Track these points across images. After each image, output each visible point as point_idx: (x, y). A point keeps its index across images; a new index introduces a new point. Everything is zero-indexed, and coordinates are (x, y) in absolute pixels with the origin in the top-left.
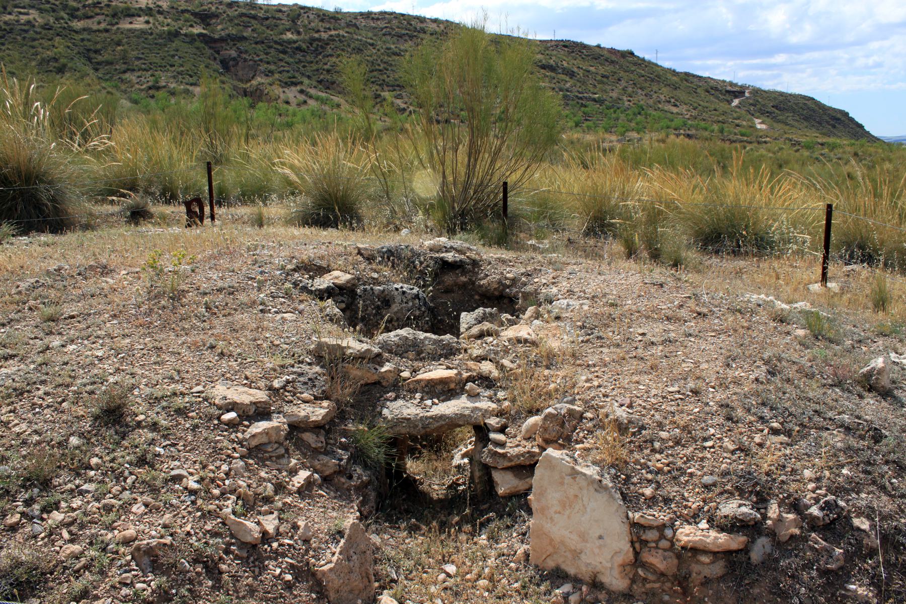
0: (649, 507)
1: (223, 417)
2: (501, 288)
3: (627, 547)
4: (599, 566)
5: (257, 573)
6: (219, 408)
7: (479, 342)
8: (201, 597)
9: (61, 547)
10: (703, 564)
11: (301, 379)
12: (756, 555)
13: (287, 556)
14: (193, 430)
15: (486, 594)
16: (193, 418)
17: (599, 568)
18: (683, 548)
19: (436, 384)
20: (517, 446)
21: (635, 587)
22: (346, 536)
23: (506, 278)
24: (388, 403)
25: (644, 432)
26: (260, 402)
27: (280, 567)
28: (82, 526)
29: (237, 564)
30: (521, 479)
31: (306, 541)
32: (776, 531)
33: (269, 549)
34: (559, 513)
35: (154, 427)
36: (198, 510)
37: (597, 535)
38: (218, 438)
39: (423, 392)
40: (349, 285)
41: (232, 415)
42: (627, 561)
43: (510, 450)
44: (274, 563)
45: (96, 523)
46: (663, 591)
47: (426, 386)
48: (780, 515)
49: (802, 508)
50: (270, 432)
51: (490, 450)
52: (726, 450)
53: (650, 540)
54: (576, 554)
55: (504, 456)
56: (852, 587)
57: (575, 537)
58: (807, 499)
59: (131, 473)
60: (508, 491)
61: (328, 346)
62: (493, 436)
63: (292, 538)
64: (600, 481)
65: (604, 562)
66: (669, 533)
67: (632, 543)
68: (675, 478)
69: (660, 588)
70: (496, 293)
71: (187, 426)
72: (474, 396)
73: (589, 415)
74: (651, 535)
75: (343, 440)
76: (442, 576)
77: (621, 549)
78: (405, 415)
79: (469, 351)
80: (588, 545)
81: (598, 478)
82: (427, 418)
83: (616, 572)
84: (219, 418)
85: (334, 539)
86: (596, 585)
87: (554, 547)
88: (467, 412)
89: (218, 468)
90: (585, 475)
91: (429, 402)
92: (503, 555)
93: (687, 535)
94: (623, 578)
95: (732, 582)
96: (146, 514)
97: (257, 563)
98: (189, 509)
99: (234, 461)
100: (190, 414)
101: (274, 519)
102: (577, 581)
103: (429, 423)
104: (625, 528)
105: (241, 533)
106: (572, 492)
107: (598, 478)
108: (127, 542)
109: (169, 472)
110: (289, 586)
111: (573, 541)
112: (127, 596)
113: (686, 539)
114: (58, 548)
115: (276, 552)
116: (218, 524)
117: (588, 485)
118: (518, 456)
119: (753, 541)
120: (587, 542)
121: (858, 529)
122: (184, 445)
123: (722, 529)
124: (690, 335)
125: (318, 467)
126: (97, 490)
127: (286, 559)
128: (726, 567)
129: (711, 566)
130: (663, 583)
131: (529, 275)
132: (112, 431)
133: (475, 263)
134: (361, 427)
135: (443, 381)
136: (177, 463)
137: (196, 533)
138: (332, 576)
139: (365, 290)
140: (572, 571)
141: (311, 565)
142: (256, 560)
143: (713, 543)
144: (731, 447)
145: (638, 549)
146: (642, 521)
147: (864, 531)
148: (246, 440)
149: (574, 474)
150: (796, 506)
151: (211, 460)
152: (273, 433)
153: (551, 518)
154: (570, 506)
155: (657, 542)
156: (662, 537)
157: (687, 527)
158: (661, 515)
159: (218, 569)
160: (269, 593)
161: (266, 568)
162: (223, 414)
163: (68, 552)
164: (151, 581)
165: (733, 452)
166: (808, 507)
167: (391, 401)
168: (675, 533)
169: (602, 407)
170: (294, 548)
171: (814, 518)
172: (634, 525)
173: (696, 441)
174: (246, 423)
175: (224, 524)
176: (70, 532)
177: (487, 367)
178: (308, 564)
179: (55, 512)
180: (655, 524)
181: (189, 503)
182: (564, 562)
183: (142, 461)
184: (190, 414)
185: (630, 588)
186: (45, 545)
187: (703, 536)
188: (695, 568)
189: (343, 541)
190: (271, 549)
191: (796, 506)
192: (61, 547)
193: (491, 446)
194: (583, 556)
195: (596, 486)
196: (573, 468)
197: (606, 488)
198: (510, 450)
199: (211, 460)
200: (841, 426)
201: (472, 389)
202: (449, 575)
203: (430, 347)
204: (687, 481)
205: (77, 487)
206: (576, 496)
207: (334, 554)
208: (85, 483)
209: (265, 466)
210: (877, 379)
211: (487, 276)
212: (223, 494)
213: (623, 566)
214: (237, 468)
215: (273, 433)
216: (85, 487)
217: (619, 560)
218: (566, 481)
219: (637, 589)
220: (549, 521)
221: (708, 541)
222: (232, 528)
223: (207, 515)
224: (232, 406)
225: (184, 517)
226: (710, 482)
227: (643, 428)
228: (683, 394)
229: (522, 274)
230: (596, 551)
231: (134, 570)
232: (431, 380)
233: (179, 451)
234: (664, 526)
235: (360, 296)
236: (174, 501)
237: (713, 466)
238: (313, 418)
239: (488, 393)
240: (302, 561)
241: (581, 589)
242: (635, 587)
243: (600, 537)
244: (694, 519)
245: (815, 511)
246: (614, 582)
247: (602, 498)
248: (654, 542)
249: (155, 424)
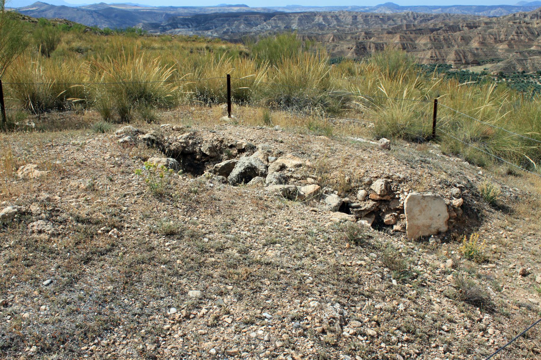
54: (429, 226)
57: (428, 220)
83: (444, 225)
86: (438, 233)
106: (424, 205)
111: (427, 222)
149: (424, 197)
154: (424, 210)
185: (448, 228)
194: (433, 226)
196: (423, 196)
217: (446, 220)
229: (187, 138)
243: (439, 215)
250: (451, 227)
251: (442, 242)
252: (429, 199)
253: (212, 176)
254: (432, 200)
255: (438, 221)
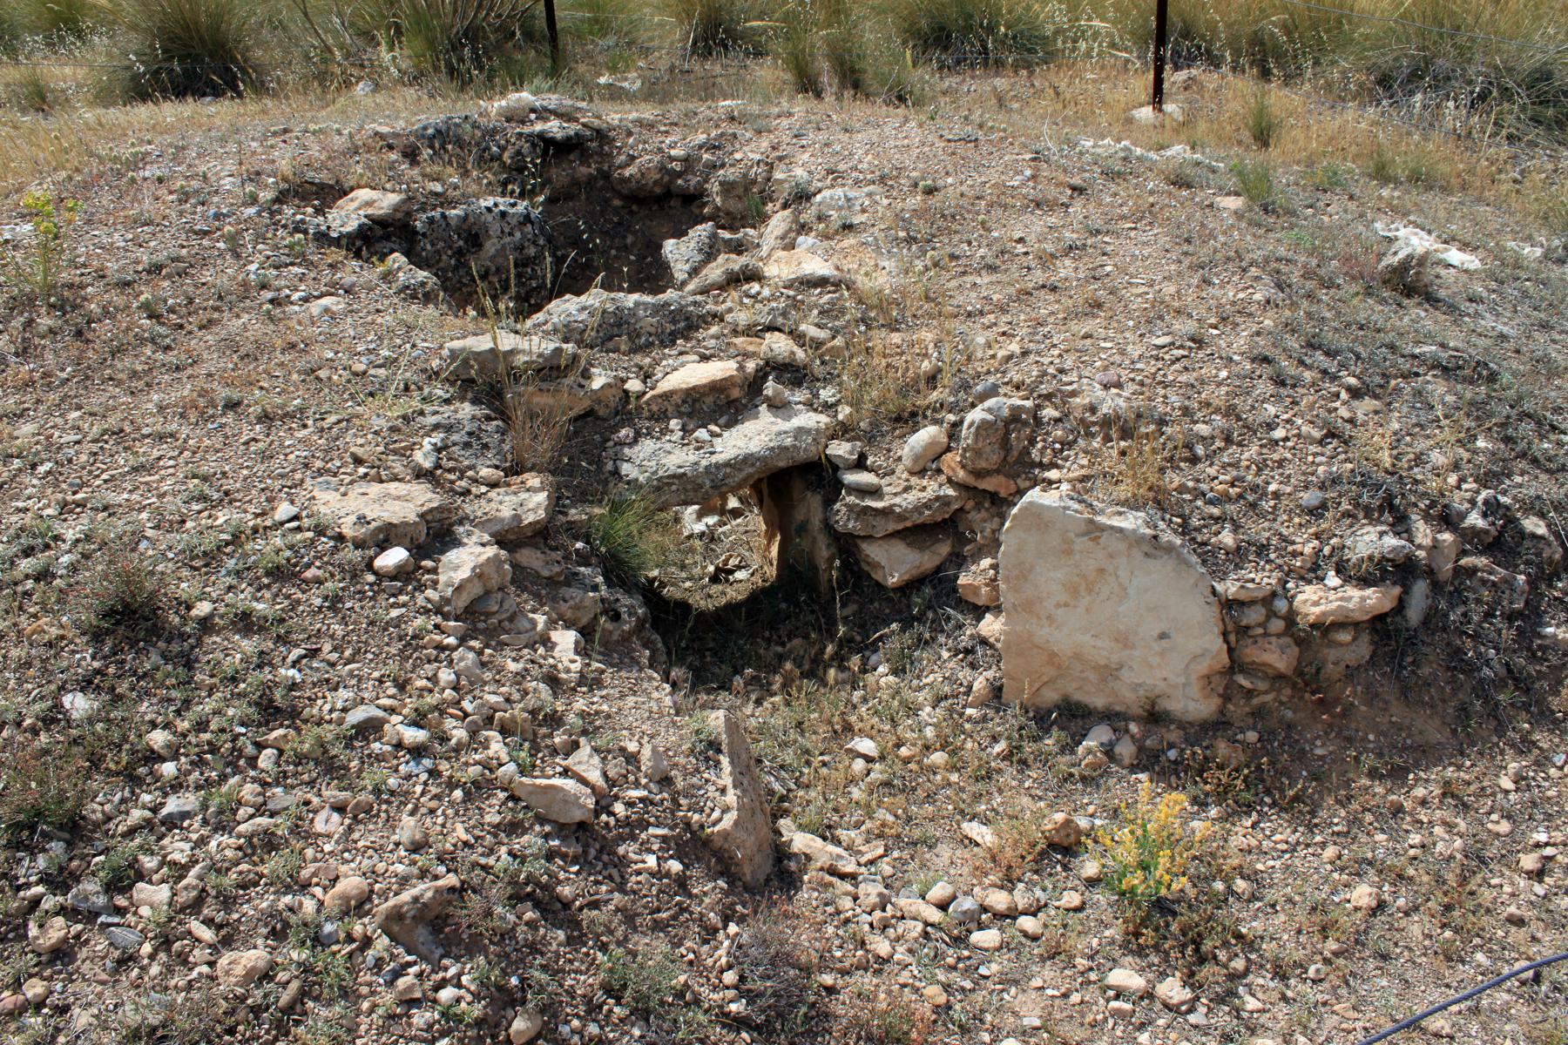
0: (1238, 567)
1: (378, 563)
2: (666, 178)
3: (1218, 645)
4: (1162, 685)
5: (618, 879)
6: (359, 544)
7: (735, 294)
8: (563, 971)
9: (211, 964)
10: (1342, 645)
11: (455, 437)
12: (1414, 614)
13: (649, 824)
14: (332, 608)
15: (954, 777)
16: (319, 582)
17: (1162, 687)
18: (1312, 626)
19: (703, 395)
20: (907, 489)
21: (1231, 707)
22: (724, 747)
23: (672, 159)
24: (626, 450)
25: (1168, 430)
26: (431, 510)
27: (650, 851)
28: (227, 902)
29: (577, 873)
30: (921, 549)
31: (665, 781)
32: (1434, 565)
33: (612, 821)
34: (1066, 605)
35: (246, 623)
36: (452, 784)
37: (1155, 633)
38: (395, 613)
39: (680, 415)
40: (399, 215)
41: (394, 557)
42: (1218, 667)
43: (897, 500)
44: (634, 847)
45: (256, 884)
46: (1281, 703)
47: (684, 402)
48: (1435, 539)
49: (1456, 520)
50: (487, 570)
51: (850, 508)
52: (1310, 440)
53: (1253, 623)
54: (1109, 672)
55: (886, 512)
56: (1550, 630)
58: (1458, 501)
59: (260, 746)
60: (906, 577)
61: (478, 355)
62: (851, 478)
63: (637, 785)
64: (1155, 537)
65: (1171, 676)
66: (1281, 605)
67: (1225, 634)
68: (1253, 506)
69: (1275, 700)
70: (658, 190)
71: (318, 602)
72: (779, 407)
73: (1049, 412)
74: (1254, 616)
75: (579, 545)
76: (859, 765)
77: (1206, 650)
78: (673, 470)
79: (728, 318)
80: (1136, 653)
81: (1149, 531)
82: (718, 466)
83: (1195, 690)
84: (370, 566)
85: (707, 759)
86: (1155, 717)
87: (1059, 667)
88: (789, 441)
89: (433, 679)
90: (1121, 530)
91: (702, 434)
92: (946, 697)
93: (1316, 603)
94: (1206, 697)
95: (1387, 664)
96: (350, 829)
97: (605, 857)
98: (434, 790)
99: (456, 655)
100: (309, 574)
101: (591, 756)
102: (1112, 717)
103: (726, 476)
104: (1214, 611)
105: (555, 808)
106: (1091, 565)
107: (1149, 531)
108: (358, 906)
109: (340, 722)
110: (682, 883)
111: (1103, 650)
112: (430, 1026)
113: (1317, 610)
114: (205, 969)
115: (627, 822)
116: (504, 803)
117: (1130, 547)
118: (918, 509)
119: (1406, 591)
120: (1133, 647)
121: (1534, 536)
122: (335, 649)
123: (1365, 581)
124: (1098, 232)
125: (569, 614)
126: (204, 807)
127: (651, 830)
128: (1372, 642)
129: (1353, 647)
130: (1279, 690)
131: (715, 147)
132: (155, 658)
133: (601, 135)
134: (597, 511)
135: (717, 387)
136: (343, 694)
137: (477, 838)
138: (741, 835)
139: (431, 221)
140: (1098, 701)
141: (695, 827)
142: (601, 851)
143: (1360, 609)
144: (1317, 434)
145: (1233, 645)
146: (1243, 596)
147: (1542, 538)
148: (447, 601)
149: (1094, 530)
150: (1447, 519)
151: (409, 666)
152: (491, 572)
153: (1049, 617)
155: (1263, 625)
156: (1272, 614)
157: (1308, 588)
158: (1263, 578)
159: (558, 899)
160: (658, 910)
161: (623, 862)
162: (377, 555)
163: (239, 970)
164: (459, 975)
165: (1321, 442)
166: (1463, 516)
167: (630, 445)
168: (1291, 603)
169: (1074, 394)
170: (652, 803)
171: (1475, 532)
172: (1229, 605)
173: (1255, 433)
174: (428, 563)
175: (513, 798)
176: (209, 922)
177: (779, 345)
178: (688, 825)
179: (140, 885)
180: (1260, 595)
181: (424, 777)
182: (1079, 688)
183: (269, 711)
184: (309, 574)
185: (1222, 712)
186: (169, 970)
187: (1341, 599)
188: (1332, 654)
189: (725, 761)
190: (617, 820)
191: (1447, 519)
192: (211, 964)
193: (851, 499)
194: (1125, 674)
195: (1146, 548)
196: (1091, 521)
197: (1169, 549)
198: (897, 500)
199: (409, 666)
200: (1433, 367)
201: (777, 394)
202: (869, 759)
203: (649, 322)
204: (1274, 507)
205: (155, 810)
206: (1102, 571)
207: (723, 791)
208: (166, 795)
209: (502, 645)
210: (1417, 273)
211: (633, 158)
212: (473, 734)
213: (1208, 678)
214: (467, 668)
215: (491, 572)
216: (172, 805)
217: (1203, 667)
218: (1077, 547)
219: (1237, 710)
220: (1044, 622)
221: (1351, 606)
222: (533, 801)
223: (478, 790)
224: (386, 536)
225: (432, 811)
226: (1316, 503)
227: (1162, 422)
228: (1182, 347)
229: (700, 147)
230: (1155, 660)
231: (410, 964)
232: (694, 388)
233: (333, 665)
234: (1274, 594)
235: (424, 235)
236: (393, 782)
237: (1304, 474)
238: (530, 518)
239: (800, 395)
240: (676, 825)
241: (1127, 731)
242: (1231, 707)
243: (1163, 636)
244: (1313, 573)
245: (1475, 519)
246: (1192, 706)
247: (1161, 569)
248: (1259, 625)
249: (246, 616)
250: (1237, 710)
251: (1134, 769)
252: (1122, 546)
253: (399, 269)
254: (1137, 554)
255: (1155, 660)
